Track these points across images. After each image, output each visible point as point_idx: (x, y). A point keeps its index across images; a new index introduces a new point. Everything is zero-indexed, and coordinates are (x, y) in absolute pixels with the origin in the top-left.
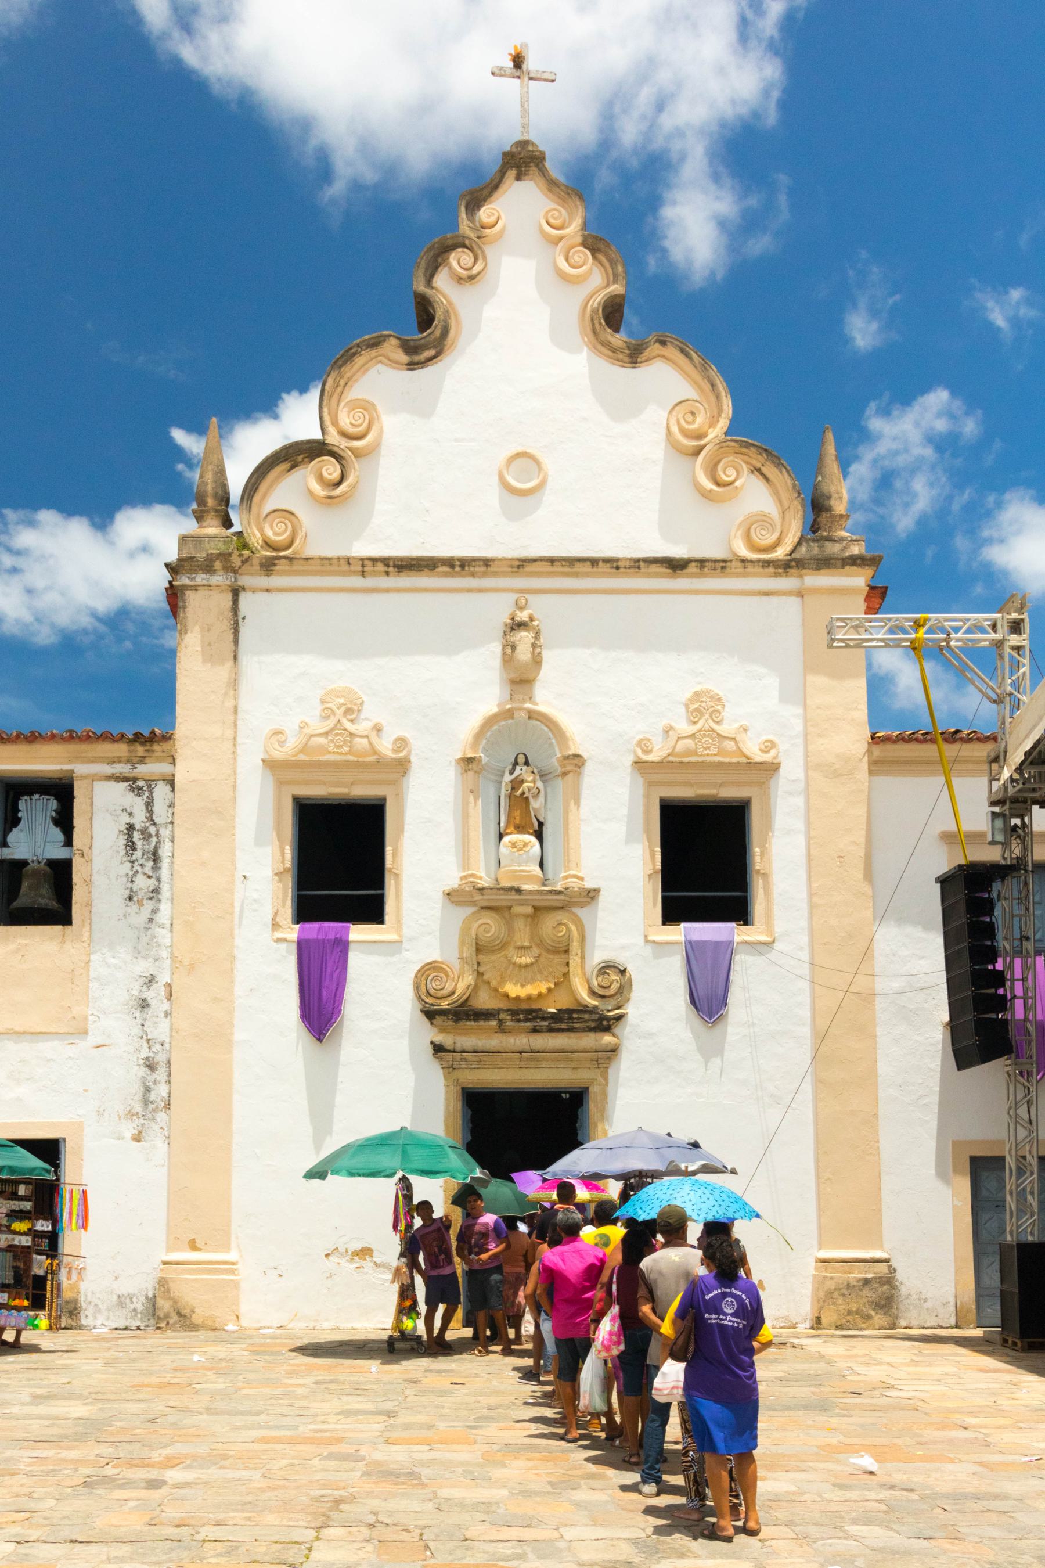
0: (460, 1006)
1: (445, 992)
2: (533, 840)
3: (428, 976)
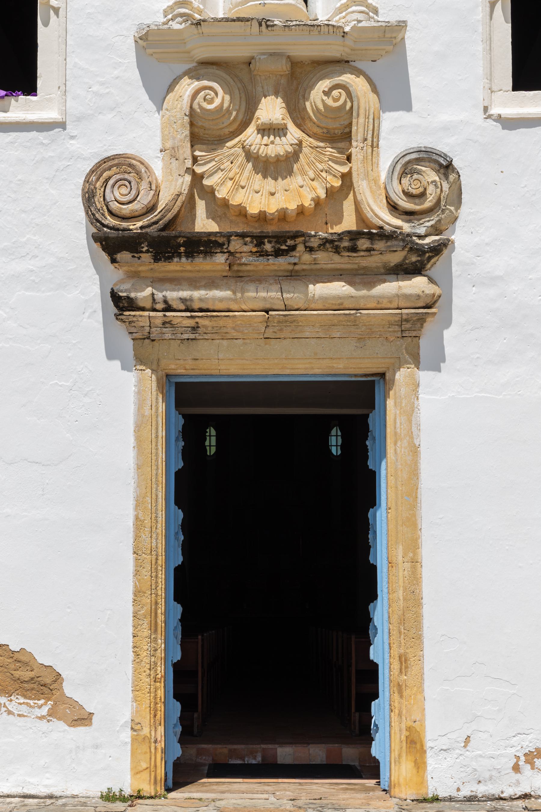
0: (163, 229)
1: (136, 206)
3: (110, 178)
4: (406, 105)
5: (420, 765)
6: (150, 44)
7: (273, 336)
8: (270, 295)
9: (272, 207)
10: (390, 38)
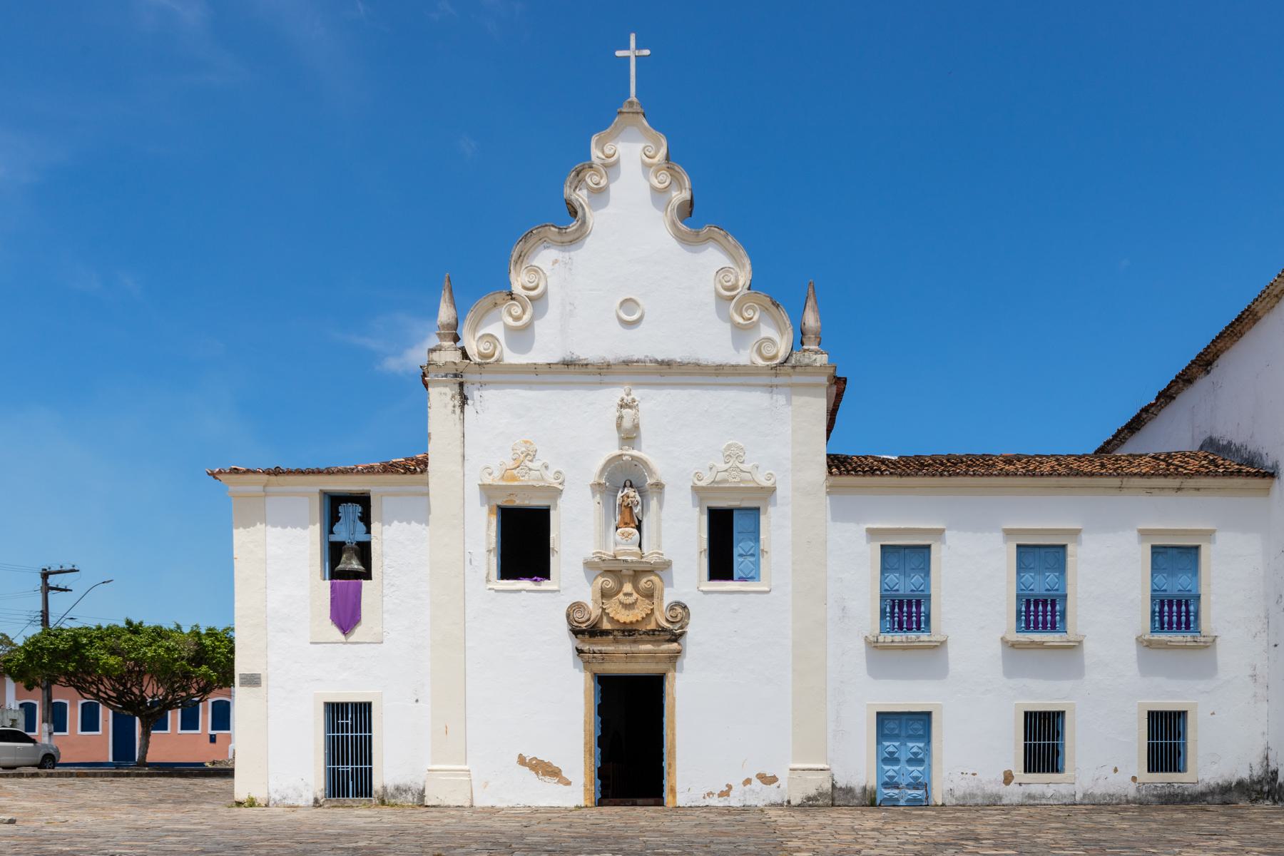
2: (635, 531)
4: (671, 585)
5: (674, 797)
6: (588, 565)
7: (630, 660)
8: (627, 648)
9: (628, 621)
10: (667, 565)
